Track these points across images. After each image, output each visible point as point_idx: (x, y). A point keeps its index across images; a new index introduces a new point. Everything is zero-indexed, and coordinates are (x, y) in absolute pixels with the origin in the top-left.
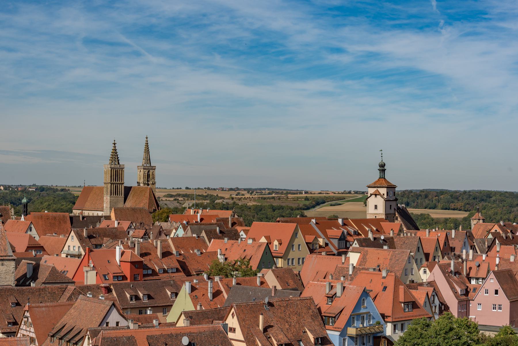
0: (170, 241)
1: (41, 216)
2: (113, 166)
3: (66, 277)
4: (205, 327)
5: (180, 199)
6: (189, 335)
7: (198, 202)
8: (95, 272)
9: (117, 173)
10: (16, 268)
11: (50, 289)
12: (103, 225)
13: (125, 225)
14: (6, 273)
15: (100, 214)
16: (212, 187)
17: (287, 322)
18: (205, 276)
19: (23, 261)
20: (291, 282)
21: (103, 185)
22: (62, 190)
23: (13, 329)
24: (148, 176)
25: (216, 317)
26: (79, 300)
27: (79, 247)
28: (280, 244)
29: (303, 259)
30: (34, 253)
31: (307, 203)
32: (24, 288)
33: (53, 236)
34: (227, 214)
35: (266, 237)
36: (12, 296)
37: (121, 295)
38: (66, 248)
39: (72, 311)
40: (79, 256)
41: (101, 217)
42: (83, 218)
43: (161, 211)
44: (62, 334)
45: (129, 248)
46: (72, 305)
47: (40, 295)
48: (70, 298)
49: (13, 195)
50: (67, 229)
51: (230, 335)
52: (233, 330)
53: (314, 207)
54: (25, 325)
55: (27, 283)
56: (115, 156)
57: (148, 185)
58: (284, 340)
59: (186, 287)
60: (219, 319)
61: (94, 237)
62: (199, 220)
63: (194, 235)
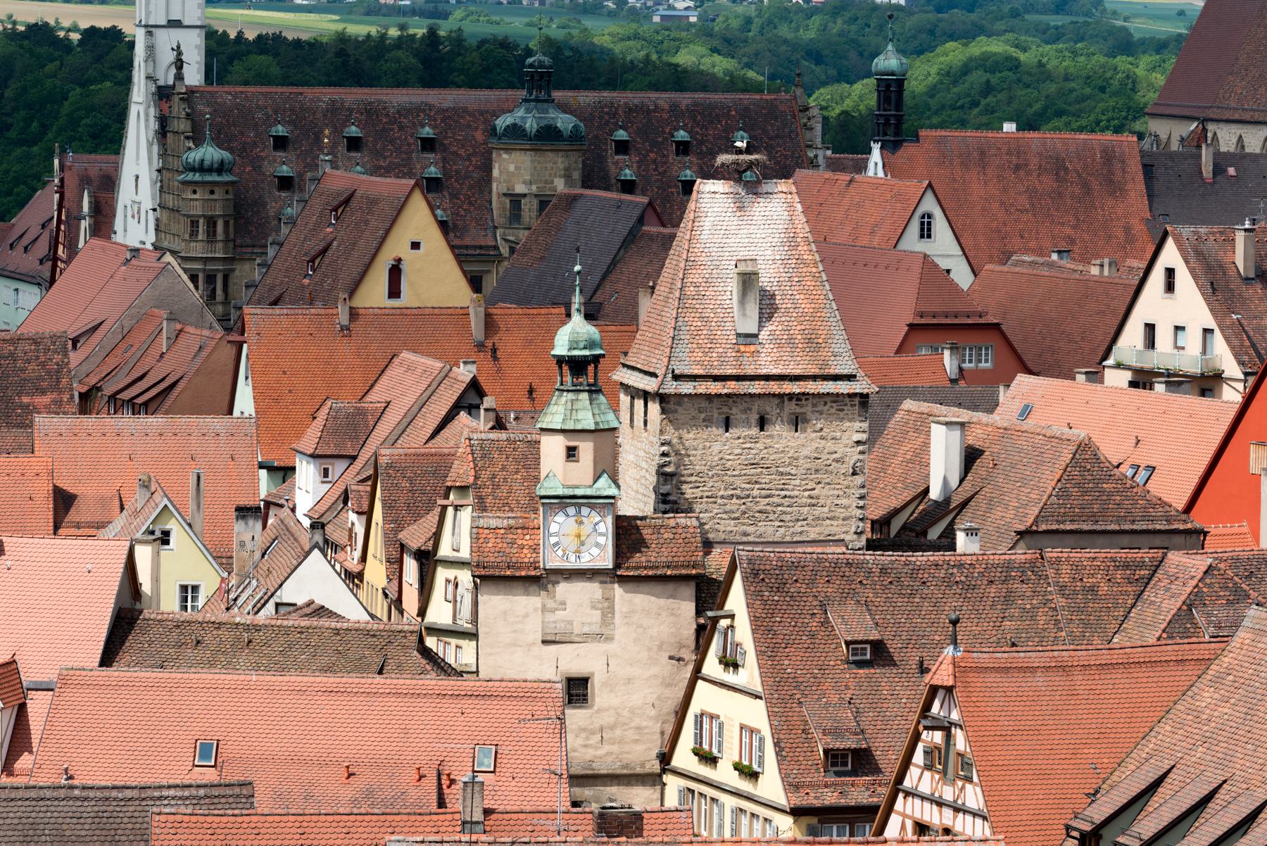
1: (983, 153)
3: (1154, 506)
11: (1065, 569)
14: (819, 469)
19: (908, 404)
27: (1207, 331)
30: (948, 359)
32: (920, 558)
33: (1051, 265)
36: (851, 606)
38: (1132, 336)
39: (1206, 696)
40: (1208, 383)
42: (1219, 169)
46: (1207, 662)
47: (1008, 599)
49: (784, 31)
50: (1128, 229)
54: (929, 767)
55: (934, 534)
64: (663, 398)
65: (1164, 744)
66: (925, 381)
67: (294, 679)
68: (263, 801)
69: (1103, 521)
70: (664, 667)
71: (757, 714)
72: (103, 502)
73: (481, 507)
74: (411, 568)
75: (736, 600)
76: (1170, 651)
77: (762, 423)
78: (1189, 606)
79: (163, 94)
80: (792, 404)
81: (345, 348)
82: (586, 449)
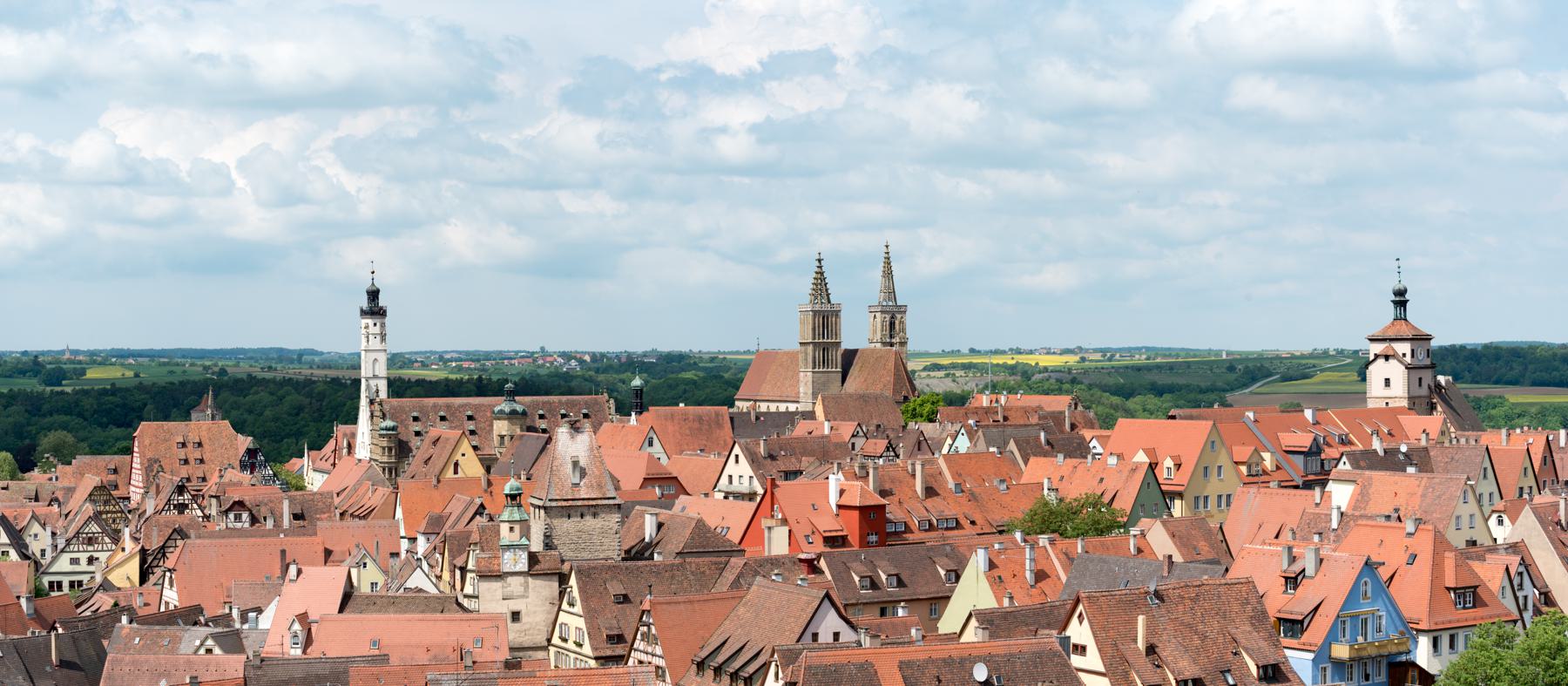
0: (941, 462)
2: (817, 307)
4: (1021, 643)
5: (958, 373)
6: (988, 660)
7: (996, 379)
8: (786, 529)
9: (825, 320)
10: (622, 523)
12: (801, 429)
13: (847, 429)
14: (603, 532)
15: (792, 407)
16: (1023, 347)
17: (1196, 632)
18: (1018, 536)
20: (1203, 546)
21: (798, 347)
22: (712, 359)
23: (619, 650)
24: (892, 325)
25: (1044, 621)
26: (754, 588)
28: (1178, 466)
29: (1229, 496)
31: (1232, 377)
34: (1059, 403)
35: (1147, 451)
37: (841, 575)
38: (724, 480)
39: (741, 610)
40: (751, 496)
41: (796, 413)
42: (757, 418)
43: (919, 401)
44: (721, 658)
45: (857, 478)
47: (673, 577)
48: (736, 584)
51: (1076, 661)
52: (1081, 650)
53: (1246, 385)
56: (821, 285)
57: (892, 345)
58: (1190, 671)
59: (979, 560)
60: (1049, 626)
61: (783, 456)
62: (1000, 418)
63: (992, 449)
64: (545, 508)
65: (727, 628)
66: (650, 498)
67: (407, 616)
68: (394, 660)
69: (707, 548)
70: (548, 606)
71: (581, 623)
72: (343, 553)
73: (482, 550)
74: (458, 573)
75: (573, 581)
76: (730, 594)
77: (582, 516)
78: (738, 577)
79: (372, 402)
80: (592, 509)
81: (436, 493)
82: (517, 527)
